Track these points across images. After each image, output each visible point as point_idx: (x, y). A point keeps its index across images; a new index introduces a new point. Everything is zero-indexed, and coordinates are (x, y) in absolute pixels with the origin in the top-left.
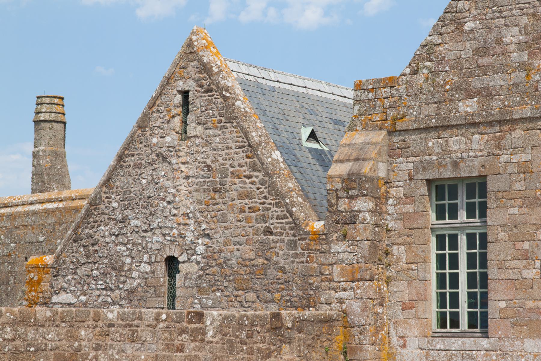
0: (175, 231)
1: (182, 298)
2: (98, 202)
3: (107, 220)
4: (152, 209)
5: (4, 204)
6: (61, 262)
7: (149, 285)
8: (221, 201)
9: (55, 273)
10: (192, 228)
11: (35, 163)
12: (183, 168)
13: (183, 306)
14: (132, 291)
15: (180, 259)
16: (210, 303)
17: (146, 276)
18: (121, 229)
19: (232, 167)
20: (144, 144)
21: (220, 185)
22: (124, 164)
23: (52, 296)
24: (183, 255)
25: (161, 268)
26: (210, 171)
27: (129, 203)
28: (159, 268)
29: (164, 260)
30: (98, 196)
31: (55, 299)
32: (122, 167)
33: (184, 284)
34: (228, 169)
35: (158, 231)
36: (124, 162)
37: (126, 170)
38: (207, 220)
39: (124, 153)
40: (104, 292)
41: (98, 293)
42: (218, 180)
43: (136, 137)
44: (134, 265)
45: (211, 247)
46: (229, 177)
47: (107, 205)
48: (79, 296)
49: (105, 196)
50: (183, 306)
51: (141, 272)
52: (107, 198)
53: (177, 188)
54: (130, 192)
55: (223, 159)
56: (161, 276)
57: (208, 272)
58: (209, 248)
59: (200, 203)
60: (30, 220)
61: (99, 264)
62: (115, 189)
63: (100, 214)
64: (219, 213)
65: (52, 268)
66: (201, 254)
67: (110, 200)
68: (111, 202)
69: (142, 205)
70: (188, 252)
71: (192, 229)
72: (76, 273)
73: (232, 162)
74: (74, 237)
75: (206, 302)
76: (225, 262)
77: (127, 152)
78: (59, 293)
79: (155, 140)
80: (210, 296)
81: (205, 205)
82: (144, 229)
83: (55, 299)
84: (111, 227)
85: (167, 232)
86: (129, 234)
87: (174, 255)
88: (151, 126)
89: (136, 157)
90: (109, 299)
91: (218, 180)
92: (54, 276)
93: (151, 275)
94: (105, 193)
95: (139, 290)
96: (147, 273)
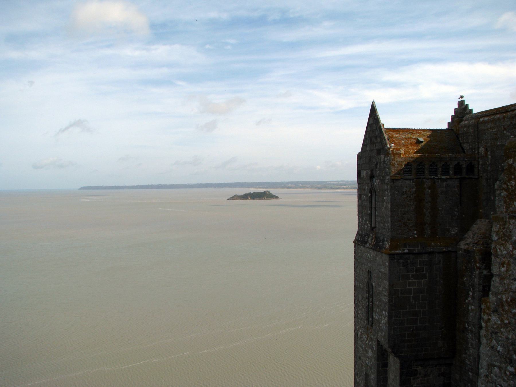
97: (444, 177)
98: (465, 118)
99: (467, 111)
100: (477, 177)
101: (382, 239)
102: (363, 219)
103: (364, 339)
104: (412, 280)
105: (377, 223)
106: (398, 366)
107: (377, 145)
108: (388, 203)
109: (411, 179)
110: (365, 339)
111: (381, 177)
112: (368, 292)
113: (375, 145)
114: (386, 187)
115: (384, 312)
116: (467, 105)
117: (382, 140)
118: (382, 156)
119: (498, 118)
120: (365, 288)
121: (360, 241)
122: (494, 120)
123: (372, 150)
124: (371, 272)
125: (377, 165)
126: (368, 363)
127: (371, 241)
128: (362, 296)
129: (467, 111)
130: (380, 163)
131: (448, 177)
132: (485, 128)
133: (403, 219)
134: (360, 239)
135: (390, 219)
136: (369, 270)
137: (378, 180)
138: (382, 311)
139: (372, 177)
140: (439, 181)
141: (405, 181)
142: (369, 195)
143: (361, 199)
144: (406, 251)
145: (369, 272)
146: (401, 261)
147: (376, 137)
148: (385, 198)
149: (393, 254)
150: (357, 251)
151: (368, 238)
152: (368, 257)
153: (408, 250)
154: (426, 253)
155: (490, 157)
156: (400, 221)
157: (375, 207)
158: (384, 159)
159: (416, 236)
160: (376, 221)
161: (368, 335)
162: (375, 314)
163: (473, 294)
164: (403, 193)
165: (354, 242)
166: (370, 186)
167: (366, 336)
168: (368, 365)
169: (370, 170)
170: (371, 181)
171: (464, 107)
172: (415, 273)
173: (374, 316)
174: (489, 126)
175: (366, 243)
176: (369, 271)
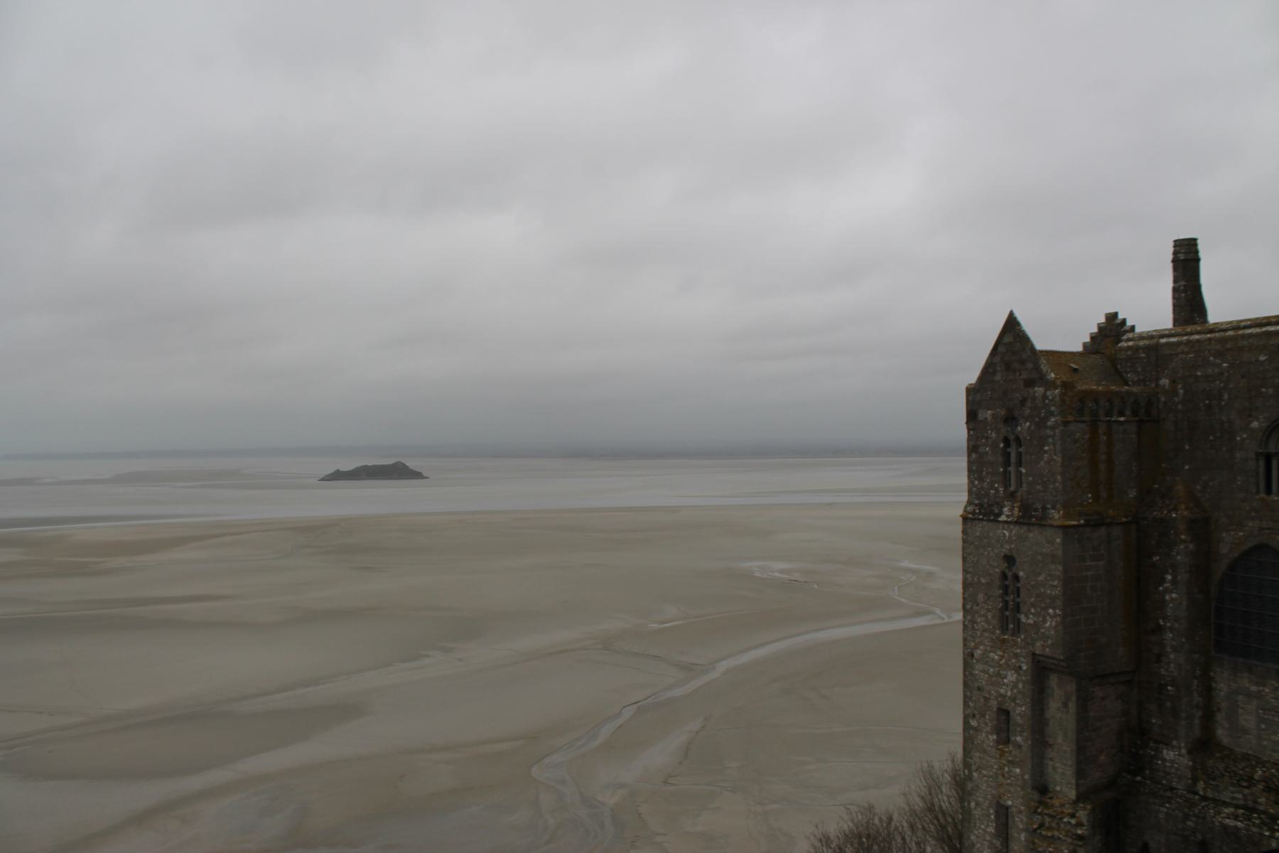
11: (1176, 296)
97: (1122, 419)
98: (1125, 337)
99: (1125, 328)
101: (1039, 507)
102: (981, 480)
103: (993, 659)
105: (1024, 485)
106: (1072, 687)
108: (1055, 454)
110: (996, 657)
111: (1037, 419)
112: (1006, 588)
113: (1018, 373)
114: (1049, 432)
115: (1051, 611)
116: (1124, 321)
117: (1040, 365)
118: (1039, 390)
119: (1198, 341)
121: (980, 513)
122: (1189, 342)
125: (1023, 402)
126: (1006, 692)
128: (986, 594)
129: (1125, 328)
130: (1034, 399)
132: (1173, 352)
134: (977, 511)
135: (1059, 478)
136: (1009, 554)
137: (1028, 424)
138: (1046, 609)
139: (1010, 419)
142: (1002, 445)
143: (976, 453)
144: (1082, 522)
145: (1009, 560)
146: (1076, 536)
147: (1023, 362)
148: (1046, 448)
151: (1003, 506)
152: (1004, 535)
153: (1084, 520)
155: (1181, 392)
158: (1045, 393)
159: (1090, 501)
161: (1004, 652)
163: (1174, 577)
165: (961, 516)
167: (1001, 653)
168: (1004, 696)
171: (1118, 321)
173: (1023, 619)
174: (1179, 350)
175: (1000, 514)
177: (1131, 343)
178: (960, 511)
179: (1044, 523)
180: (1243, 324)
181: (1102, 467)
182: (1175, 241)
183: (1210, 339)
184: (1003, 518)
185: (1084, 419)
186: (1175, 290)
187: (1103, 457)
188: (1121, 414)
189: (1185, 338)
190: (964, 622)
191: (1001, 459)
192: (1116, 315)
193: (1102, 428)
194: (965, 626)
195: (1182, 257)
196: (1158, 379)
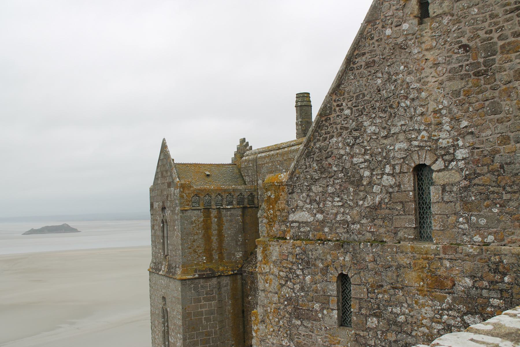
0: (424, 133)
1: (440, 216)
2: (328, 112)
3: (339, 131)
4: (392, 111)
5: (278, 147)
6: (296, 179)
7: (395, 201)
8: (489, 86)
9: (290, 191)
10: (447, 127)
11: (297, 128)
12: (429, 55)
13: (444, 226)
14: (375, 208)
15: (434, 167)
16: (483, 222)
17: (391, 190)
18: (356, 138)
19: (503, 39)
20: (376, 38)
21: (485, 66)
22: (355, 66)
23: (289, 214)
24: (437, 162)
25: (409, 179)
26: (467, 51)
27: (364, 108)
28: (406, 180)
29: (411, 170)
30: (328, 105)
31: (292, 217)
32: (352, 69)
33: (443, 198)
34: (496, 43)
35: (401, 137)
36: (354, 63)
37: (357, 72)
38: (468, 114)
39: (353, 54)
40: (342, 210)
41: (334, 211)
42: (481, 60)
43: (365, 33)
44: (374, 178)
45: (478, 148)
46: (498, 53)
47: (338, 113)
48: (315, 215)
49: (335, 104)
50: (444, 226)
51: (383, 186)
52: (338, 106)
53: (422, 81)
54: (364, 96)
55: (486, 33)
56: (409, 189)
57: (476, 181)
58: (476, 151)
59: (456, 93)
60: (292, 155)
61: (334, 179)
62: (346, 95)
63: (331, 124)
64: (487, 103)
65: (287, 185)
66: (463, 159)
67: (342, 107)
68: (343, 110)
69: (379, 108)
70: (444, 157)
71: (448, 128)
72: (310, 190)
73: (500, 33)
74: (306, 152)
75: (477, 221)
76: (502, 167)
77: (356, 52)
78: (295, 211)
79: (388, 32)
80: (482, 213)
81: (465, 95)
82: (382, 134)
83: (292, 217)
84: (344, 137)
85: (413, 136)
86: (365, 143)
87: (425, 163)
88: (382, 17)
89: (367, 55)
90: (349, 217)
91: (481, 60)
92: (290, 194)
93: (397, 189)
94: (335, 101)
95: (383, 206)
96: (391, 187)
97: (229, 207)
98: (245, 154)
100: (257, 206)
102: (156, 247)
104: (203, 302)
107: (167, 178)
109: (198, 210)
112: (164, 317)
114: (176, 217)
115: (179, 335)
119: (273, 155)
120: (161, 313)
123: (163, 183)
124: (165, 297)
125: (167, 197)
127: (164, 268)
131: (231, 206)
132: (263, 163)
133: (192, 247)
139: (164, 209)
140: (224, 210)
141: (193, 211)
142: (162, 225)
144: (197, 276)
146: (192, 286)
147: (167, 171)
148: (175, 227)
149: (185, 280)
150: (152, 279)
152: (162, 284)
153: (199, 275)
154: (214, 277)
156: (190, 248)
157: (167, 237)
159: (205, 261)
160: (168, 249)
162: (171, 337)
164: (192, 223)
166: (162, 217)
169: (161, 202)
170: (162, 212)
172: (205, 296)
173: (170, 340)
175: (160, 270)
176: (163, 297)
177: (247, 158)
178: (148, 267)
179: (174, 277)
180: (292, 143)
181: (214, 238)
182: (296, 94)
183: (277, 154)
184: (161, 273)
185: (199, 208)
186: (297, 124)
187: (215, 232)
188: (230, 203)
189: (268, 153)
190: (152, 337)
191: (161, 234)
192: (244, 139)
193: (214, 213)
194: (152, 340)
195: (299, 104)
196: (257, 180)
